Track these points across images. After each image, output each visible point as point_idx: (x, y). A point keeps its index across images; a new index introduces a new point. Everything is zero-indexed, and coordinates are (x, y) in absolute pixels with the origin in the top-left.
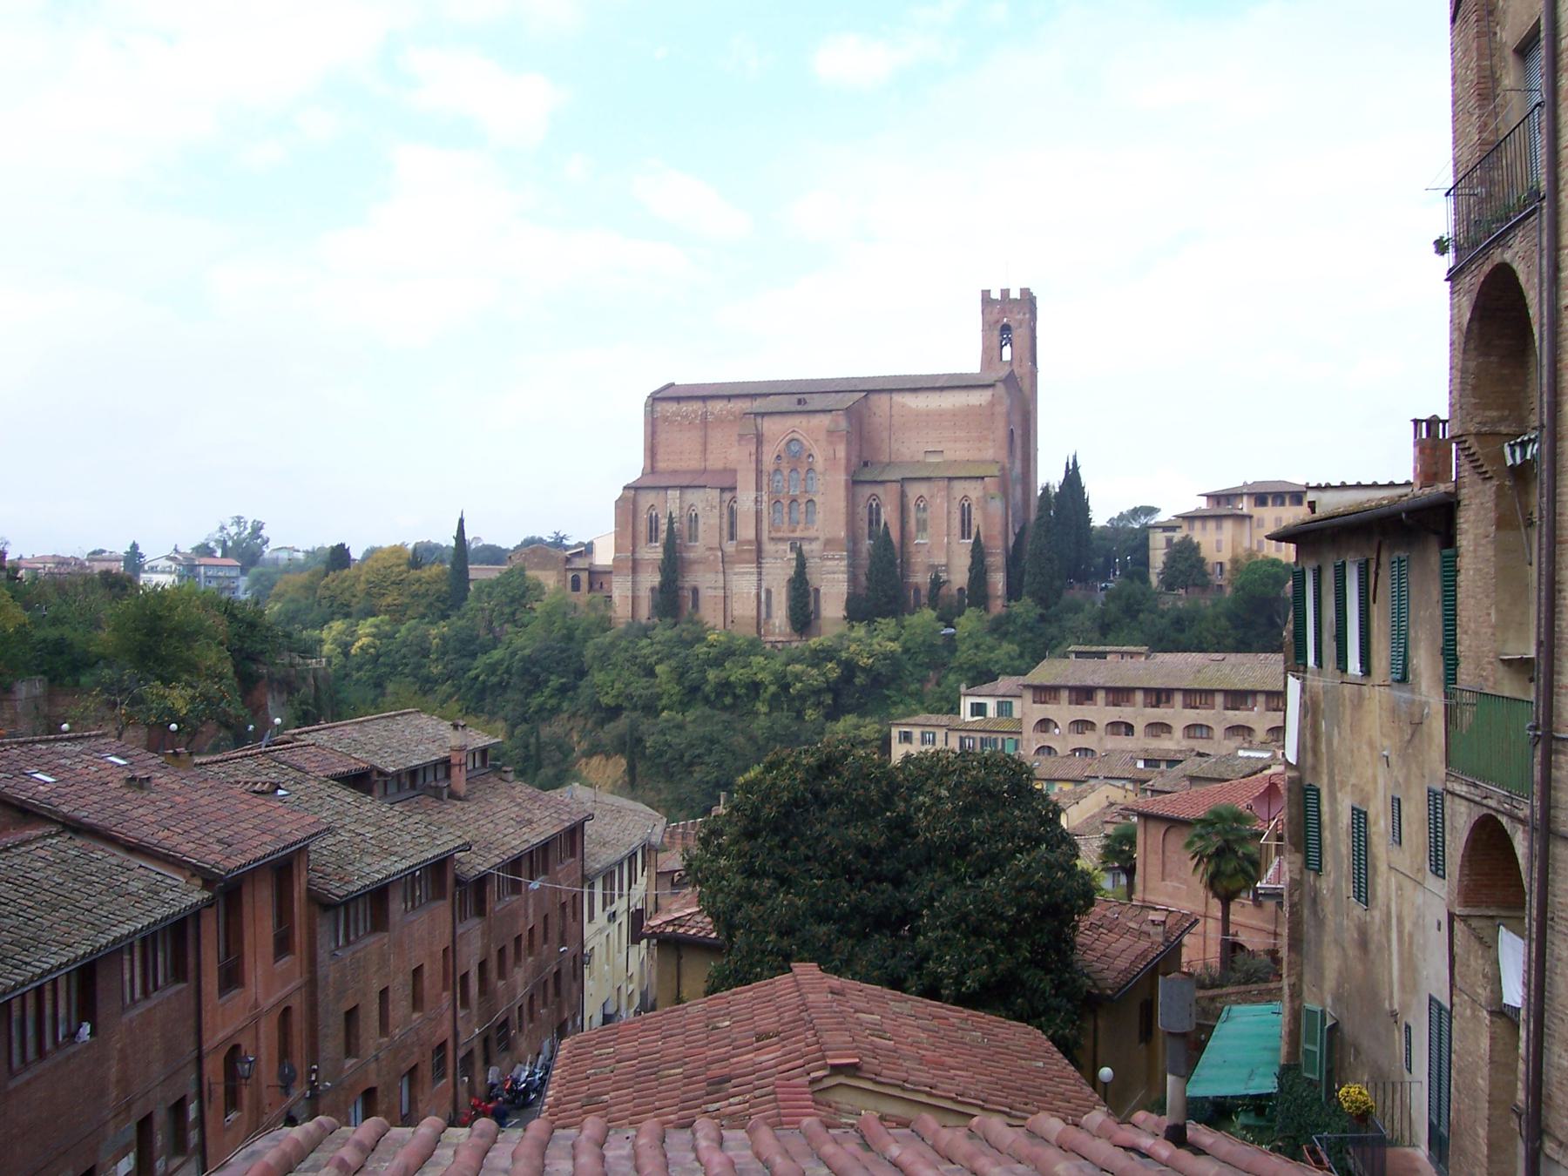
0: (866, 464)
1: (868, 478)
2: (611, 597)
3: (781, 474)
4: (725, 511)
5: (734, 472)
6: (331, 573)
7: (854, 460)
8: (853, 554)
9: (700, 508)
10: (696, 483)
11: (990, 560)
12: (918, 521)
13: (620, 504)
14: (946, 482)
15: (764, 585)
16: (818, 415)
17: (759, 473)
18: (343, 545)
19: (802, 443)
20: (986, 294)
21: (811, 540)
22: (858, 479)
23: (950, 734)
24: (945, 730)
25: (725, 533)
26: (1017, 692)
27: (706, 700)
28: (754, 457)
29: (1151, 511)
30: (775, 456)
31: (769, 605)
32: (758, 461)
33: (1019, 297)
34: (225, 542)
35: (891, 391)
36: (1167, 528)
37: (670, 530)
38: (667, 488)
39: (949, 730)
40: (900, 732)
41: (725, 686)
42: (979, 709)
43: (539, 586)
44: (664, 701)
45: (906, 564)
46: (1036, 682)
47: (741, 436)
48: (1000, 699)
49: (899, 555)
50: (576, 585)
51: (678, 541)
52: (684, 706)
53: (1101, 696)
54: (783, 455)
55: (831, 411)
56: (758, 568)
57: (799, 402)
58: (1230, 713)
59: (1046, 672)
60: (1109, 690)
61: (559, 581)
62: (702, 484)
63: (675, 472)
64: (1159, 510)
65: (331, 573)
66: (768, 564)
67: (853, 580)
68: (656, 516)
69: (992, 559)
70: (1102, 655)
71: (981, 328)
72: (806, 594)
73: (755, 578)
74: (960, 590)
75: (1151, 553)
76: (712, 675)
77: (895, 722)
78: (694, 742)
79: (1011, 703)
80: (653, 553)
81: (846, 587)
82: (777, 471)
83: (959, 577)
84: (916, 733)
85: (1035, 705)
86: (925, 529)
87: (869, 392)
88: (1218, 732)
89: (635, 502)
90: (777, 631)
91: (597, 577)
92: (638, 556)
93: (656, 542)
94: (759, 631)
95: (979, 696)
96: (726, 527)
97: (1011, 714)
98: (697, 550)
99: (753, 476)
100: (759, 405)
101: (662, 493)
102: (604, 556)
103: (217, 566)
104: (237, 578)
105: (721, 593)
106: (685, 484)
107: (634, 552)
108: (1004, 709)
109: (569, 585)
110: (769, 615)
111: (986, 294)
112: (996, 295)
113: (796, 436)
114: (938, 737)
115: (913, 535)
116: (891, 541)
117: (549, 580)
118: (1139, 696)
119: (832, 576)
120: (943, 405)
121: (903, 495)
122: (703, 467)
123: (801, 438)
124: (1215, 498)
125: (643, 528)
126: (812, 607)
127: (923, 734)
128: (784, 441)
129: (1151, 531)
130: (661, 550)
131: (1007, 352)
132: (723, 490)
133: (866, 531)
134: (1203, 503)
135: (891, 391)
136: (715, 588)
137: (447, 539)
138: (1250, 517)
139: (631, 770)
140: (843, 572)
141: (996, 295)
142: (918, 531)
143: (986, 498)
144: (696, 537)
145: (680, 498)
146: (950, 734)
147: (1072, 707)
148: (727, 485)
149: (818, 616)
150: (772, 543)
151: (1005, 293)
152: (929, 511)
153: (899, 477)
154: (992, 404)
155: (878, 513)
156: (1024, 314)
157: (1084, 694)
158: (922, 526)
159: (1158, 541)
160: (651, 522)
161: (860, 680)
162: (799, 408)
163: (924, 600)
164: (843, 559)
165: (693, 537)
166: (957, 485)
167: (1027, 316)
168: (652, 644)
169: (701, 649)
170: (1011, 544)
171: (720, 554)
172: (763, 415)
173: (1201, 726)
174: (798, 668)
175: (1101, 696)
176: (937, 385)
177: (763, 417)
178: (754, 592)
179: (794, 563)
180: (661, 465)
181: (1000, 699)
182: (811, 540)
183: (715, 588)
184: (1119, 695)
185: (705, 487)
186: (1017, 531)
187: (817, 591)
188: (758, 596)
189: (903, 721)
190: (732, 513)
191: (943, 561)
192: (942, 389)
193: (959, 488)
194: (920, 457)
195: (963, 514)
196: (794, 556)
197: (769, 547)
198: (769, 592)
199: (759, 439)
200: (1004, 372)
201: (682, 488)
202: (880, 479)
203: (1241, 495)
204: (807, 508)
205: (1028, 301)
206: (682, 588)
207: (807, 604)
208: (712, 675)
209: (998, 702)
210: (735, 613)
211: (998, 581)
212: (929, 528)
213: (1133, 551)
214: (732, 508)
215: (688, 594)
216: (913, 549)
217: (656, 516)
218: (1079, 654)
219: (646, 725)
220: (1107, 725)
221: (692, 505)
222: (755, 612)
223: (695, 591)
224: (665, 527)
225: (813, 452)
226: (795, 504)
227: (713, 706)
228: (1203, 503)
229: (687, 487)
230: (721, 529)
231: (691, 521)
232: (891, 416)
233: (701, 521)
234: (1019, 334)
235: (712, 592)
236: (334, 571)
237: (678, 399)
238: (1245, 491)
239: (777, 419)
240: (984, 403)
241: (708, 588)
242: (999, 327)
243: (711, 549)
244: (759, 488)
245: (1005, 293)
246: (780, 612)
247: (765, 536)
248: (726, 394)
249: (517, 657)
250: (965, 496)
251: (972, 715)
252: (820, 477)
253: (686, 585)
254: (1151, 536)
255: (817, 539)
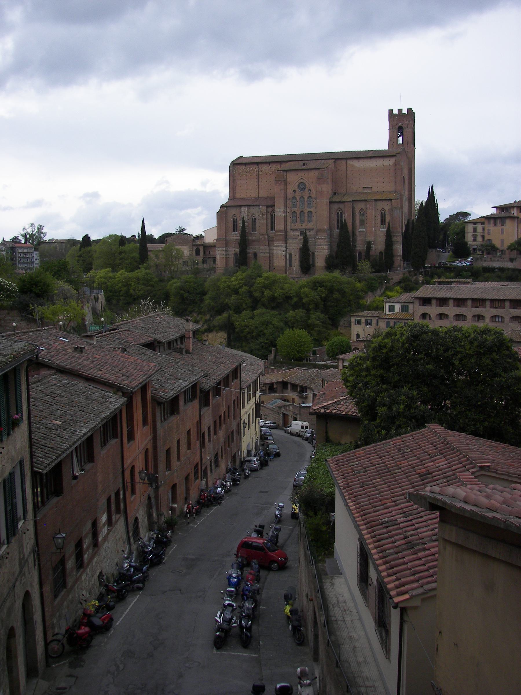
0: (335, 194)
1: (338, 200)
2: (216, 258)
3: (296, 199)
4: (269, 217)
5: (273, 199)
6: (82, 249)
7: (330, 192)
8: (331, 236)
9: (257, 215)
10: (255, 204)
11: (394, 239)
12: (360, 220)
13: (219, 214)
14: (374, 202)
15: (288, 252)
16: (313, 171)
17: (286, 198)
18: (87, 235)
19: (305, 184)
20: (391, 111)
21: (310, 230)
22: (334, 200)
23: (379, 320)
24: (376, 318)
25: (269, 227)
26: (411, 300)
27: (264, 305)
28: (283, 191)
29: (466, 214)
30: (293, 190)
31: (290, 261)
32: (285, 193)
33: (406, 113)
34: (26, 235)
35: (346, 159)
36: (475, 222)
37: (243, 226)
38: (241, 206)
39: (379, 318)
40: (355, 319)
41: (273, 299)
42: (391, 309)
43: (180, 252)
44: (244, 306)
45: (355, 240)
46: (421, 296)
47: (277, 181)
48: (403, 304)
49: (351, 236)
50: (198, 253)
51: (247, 231)
52: (254, 308)
53: (451, 302)
54: (296, 190)
55: (319, 169)
56: (285, 243)
57: (304, 164)
58: (512, 310)
59: (425, 291)
60: (455, 299)
61: (189, 251)
62: (258, 204)
63: (244, 199)
64: (470, 215)
65: (82, 249)
66: (290, 241)
67: (331, 248)
68: (236, 219)
69: (396, 238)
70: (450, 283)
71: (388, 128)
72: (309, 255)
73: (284, 248)
74: (381, 253)
75: (466, 235)
76: (267, 292)
77: (354, 315)
78: (257, 325)
79: (408, 306)
80: (235, 236)
81: (327, 252)
82: (294, 197)
83: (379, 246)
84: (363, 320)
85: (420, 307)
86: (364, 224)
87: (336, 159)
88: (507, 319)
89: (226, 213)
90: (294, 272)
91: (208, 247)
92: (228, 238)
93: (236, 232)
94: (286, 273)
95: (393, 302)
96: (269, 224)
97: (408, 311)
98: (254, 236)
99: (282, 201)
100: (285, 166)
101: (239, 208)
102: (210, 239)
103: (24, 247)
104: (33, 252)
105: (267, 255)
106: (250, 204)
107: (226, 237)
108: (405, 309)
109: (195, 252)
110: (291, 265)
111: (391, 111)
112: (396, 112)
113: (302, 181)
114: (373, 322)
115: (358, 227)
116: (347, 230)
117: (186, 251)
118: (469, 303)
119: (321, 247)
120: (372, 166)
121: (353, 208)
122: (257, 196)
123: (305, 182)
124: (501, 208)
125: (231, 225)
126: (311, 263)
127: (366, 320)
128: (297, 184)
129: (466, 224)
130: (239, 235)
131: (400, 139)
132: (268, 207)
133: (336, 226)
134: (494, 211)
135: (346, 159)
136: (265, 253)
137: (136, 231)
138: (517, 218)
139: (229, 337)
140: (325, 245)
141: (396, 112)
142: (360, 225)
143: (391, 211)
144: (255, 229)
145: (248, 211)
146: (379, 320)
147: (438, 307)
148: (269, 204)
149: (314, 265)
150: (292, 232)
151: (400, 110)
152: (365, 215)
153: (351, 200)
154: (395, 164)
155: (342, 217)
156: (409, 121)
157: (443, 301)
158: (363, 223)
159: (470, 229)
160: (234, 222)
161: (336, 295)
162: (304, 167)
163: (363, 257)
164: (325, 239)
165: (254, 229)
166: (379, 203)
167: (411, 122)
168: (237, 280)
169: (259, 280)
170: (404, 231)
171: (266, 237)
172: (286, 171)
173: (498, 316)
174: (306, 289)
175: (451, 302)
176: (369, 155)
177: (287, 172)
178: (283, 254)
179: (302, 241)
180: (238, 195)
181: (403, 304)
182: (310, 230)
183: (265, 253)
184: (460, 302)
185: (259, 205)
186: (406, 224)
187: (313, 254)
188: (286, 256)
189: (357, 314)
190: (273, 218)
191: (372, 239)
192: (371, 158)
193: (380, 205)
194: (361, 190)
195: (382, 217)
196: (302, 237)
197: (291, 233)
198: (290, 255)
199: (286, 183)
200: (399, 150)
201: (249, 206)
202: (342, 201)
203: (513, 207)
204: (308, 214)
205: (411, 113)
206: (249, 253)
207: (309, 259)
208: (267, 292)
209: (402, 305)
210: (275, 265)
211: (398, 249)
212: (365, 224)
213: (457, 234)
214: (272, 215)
215: (250, 256)
216: (357, 233)
217: (236, 219)
218: (440, 283)
219: (235, 317)
220: (454, 316)
221: (253, 214)
222: (284, 265)
223: (255, 255)
224: (241, 225)
225: (311, 189)
226: (302, 213)
227: (267, 308)
228: (494, 211)
229: (251, 205)
230: (267, 225)
231: (253, 221)
232: (347, 171)
233: (257, 221)
234: (406, 131)
235: (262, 255)
236: (84, 248)
237: (245, 164)
238: (515, 205)
239: (293, 173)
240: (391, 164)
241: (261, 253)
242: (397, 127)
243: (262, 234)
244: (285, 206)
245: (400, 110)
246: (296, 264)
247: (288, 228)
248: (267, 161)
249: (173, 287)
250: (383, 208)
251: (389, 312)
252: (314, 200)
253: (251, 252)
254: (466, 227)
255: (313, 229)
